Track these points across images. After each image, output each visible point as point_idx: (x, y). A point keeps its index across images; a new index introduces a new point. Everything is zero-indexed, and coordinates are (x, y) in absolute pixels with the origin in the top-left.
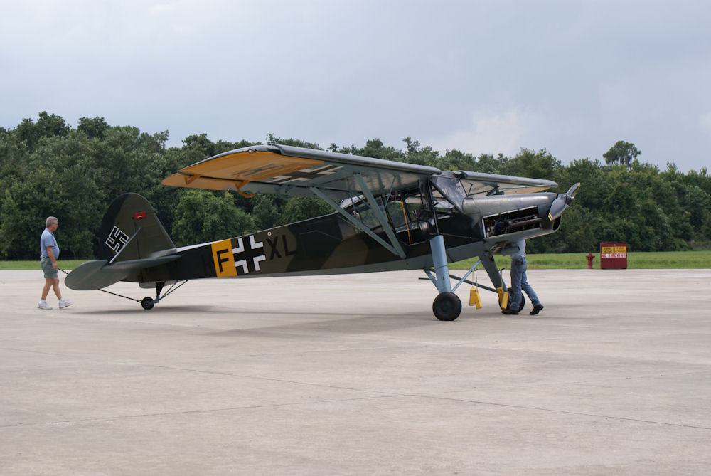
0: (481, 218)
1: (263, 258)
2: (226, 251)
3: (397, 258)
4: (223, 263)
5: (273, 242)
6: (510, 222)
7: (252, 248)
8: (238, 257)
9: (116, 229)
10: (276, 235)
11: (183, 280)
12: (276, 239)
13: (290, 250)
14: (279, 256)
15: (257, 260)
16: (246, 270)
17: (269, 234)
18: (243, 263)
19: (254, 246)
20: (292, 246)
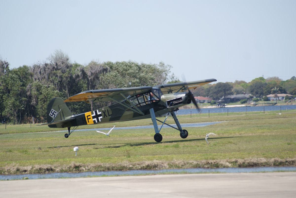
1: (101, 117)
2: (90, 115)
4: (89, 120)
5: (104, 111)
7: (98, 114)
9: (52, 110)
10: (105, 110)
11: (76, 126)
12: (105, 111)
14: (107, 116)
15: (100, 118)
16: (96, 122)
17: (103, 109)
18: (95, 119)
19: (98, 113)
20: (110, 113)
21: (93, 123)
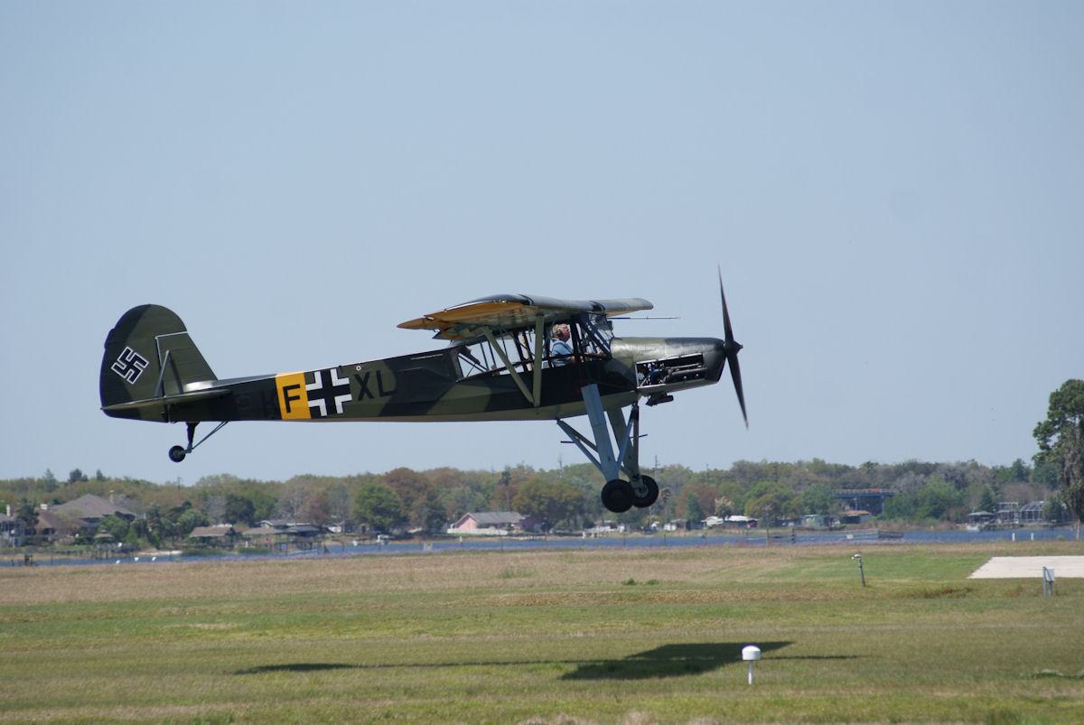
0: (633, 365)
1: (348, 397)
2: (298, 386)
3: (530, 405)
4: (292, 403)
6: (670, 371)
7: (334, 385)
8: (313, 395)
10: (368, 371)
13: (387, 388)
14: (371, 396)
15: (339, 400)
16: (324, 412)
18: (321, 403)
19: (336, 382)
20: (389, 384)
21: (309, 416)
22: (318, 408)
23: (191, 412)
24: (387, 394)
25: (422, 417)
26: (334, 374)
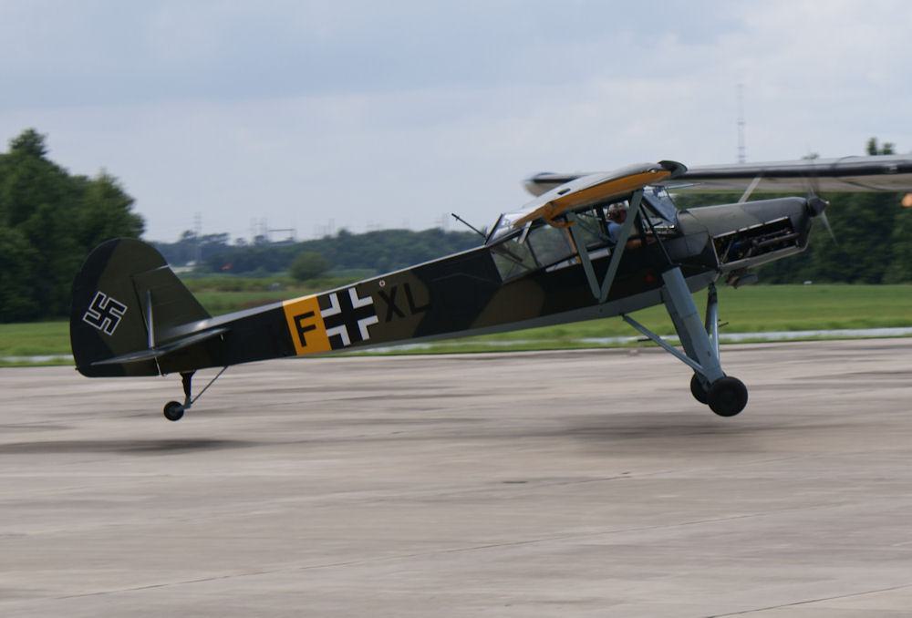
1: (374, 320)
2: (311, 314)
4: (307, 335)
5: (389, 295)
8: (331, 322)
13: (418, 304)
14: (401, 315)
15: (363, 324)
16: (346, 340)
18: (342, 330)
19: (357, 303)
20: (422, 298)
22: (339, 336)
23: (186, 361)
24: (420, 310)
25: (471, 331)
26: (353, 294)
